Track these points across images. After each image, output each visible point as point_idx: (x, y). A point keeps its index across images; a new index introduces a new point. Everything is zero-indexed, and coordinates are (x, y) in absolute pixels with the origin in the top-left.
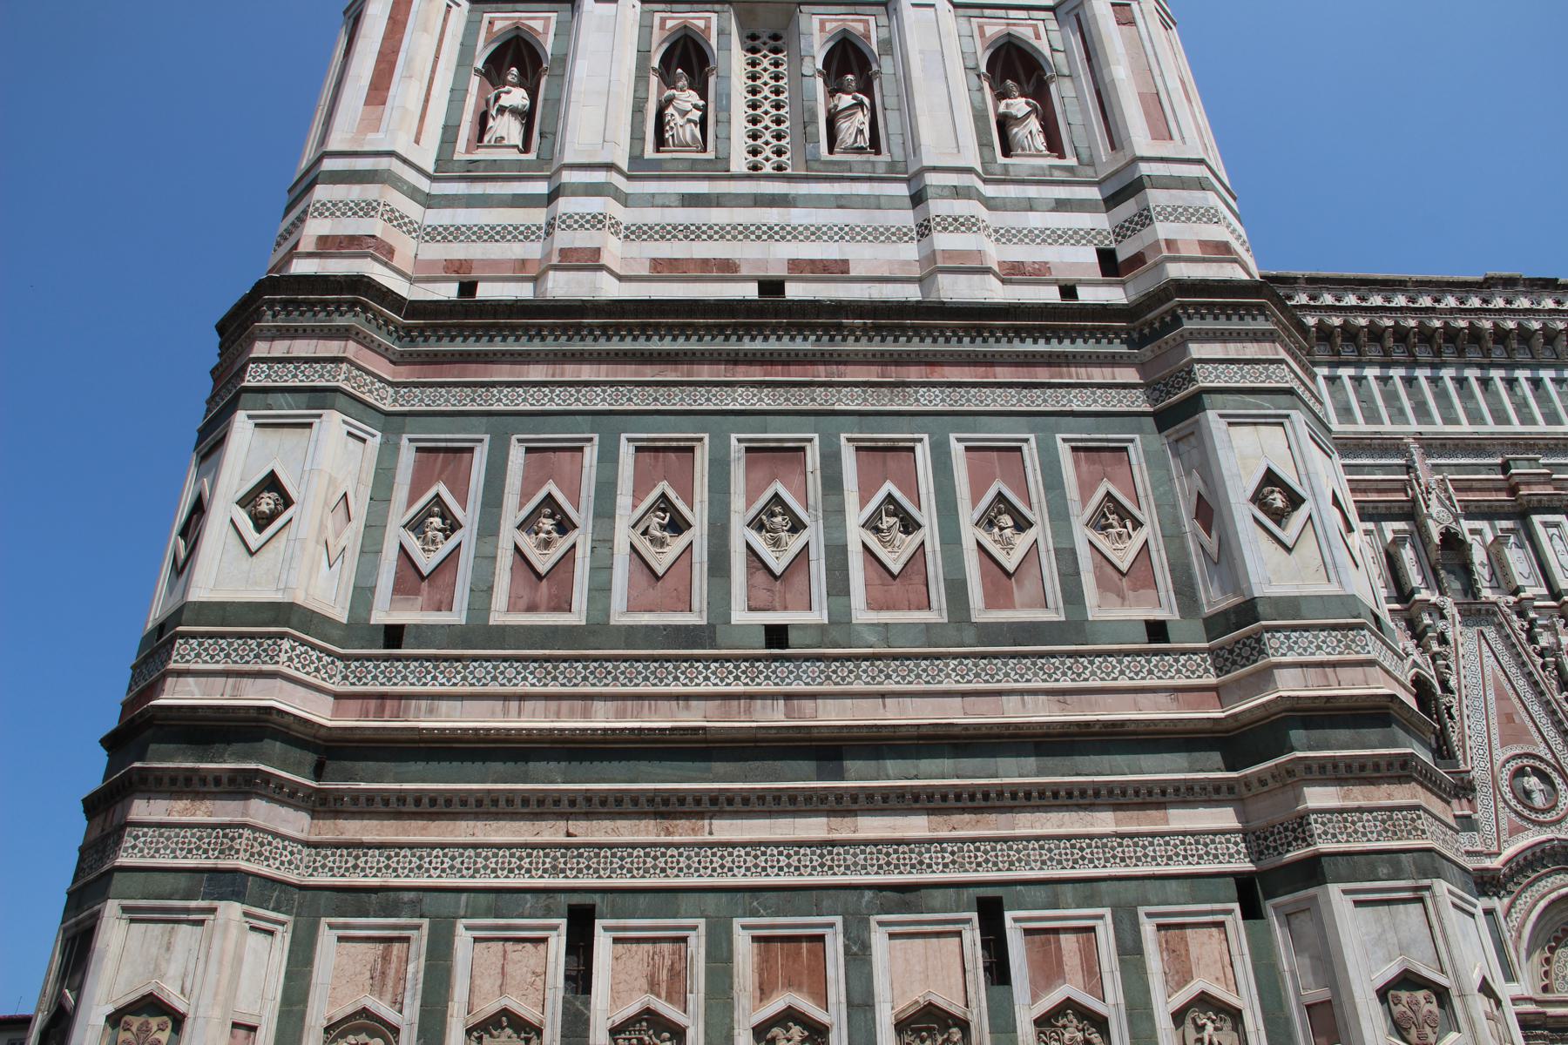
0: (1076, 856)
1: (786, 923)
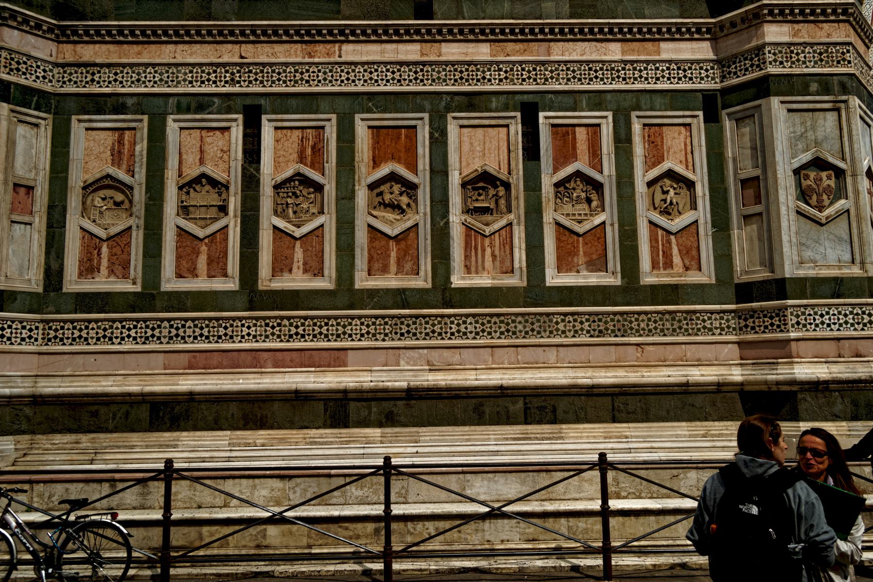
0: (592, 76)
1: (390, 119)
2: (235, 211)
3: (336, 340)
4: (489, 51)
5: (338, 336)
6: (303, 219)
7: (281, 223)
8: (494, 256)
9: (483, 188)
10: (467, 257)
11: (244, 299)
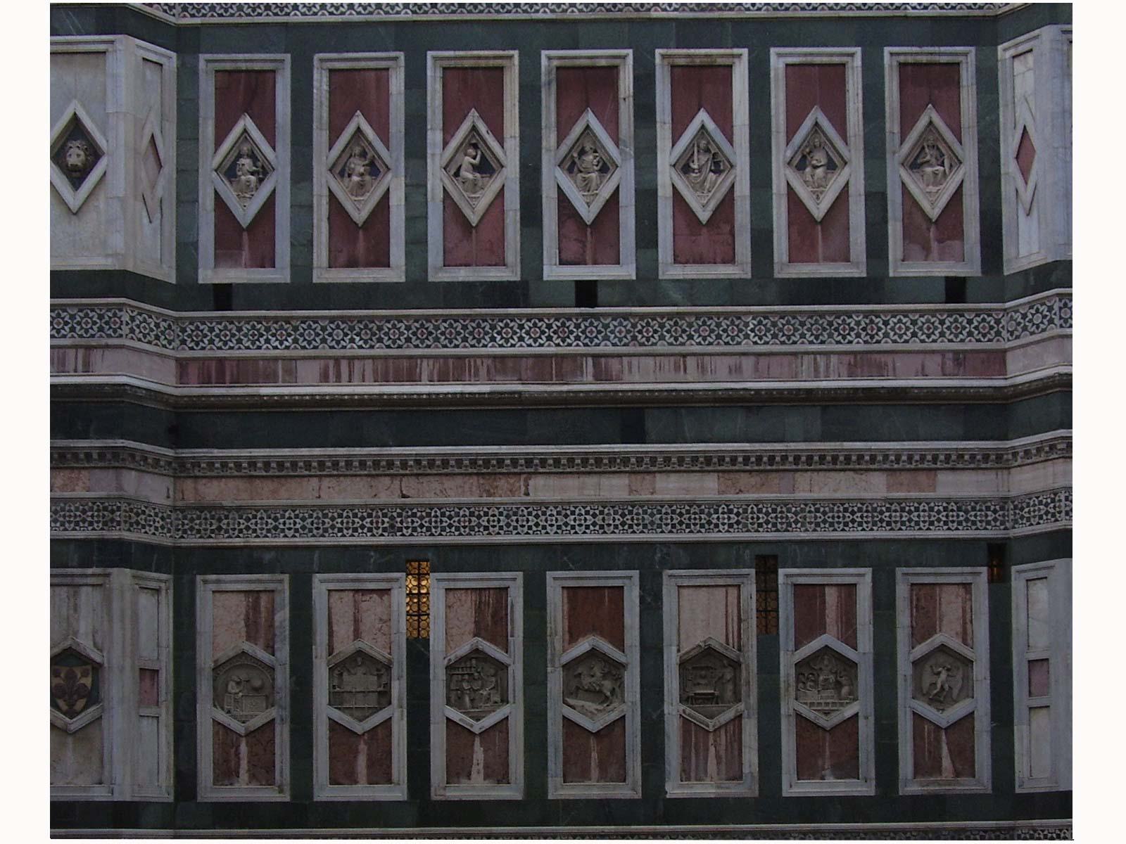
2: (400, 699)
8: (718, 757)
9: (708, 668)
10: (685, 759)
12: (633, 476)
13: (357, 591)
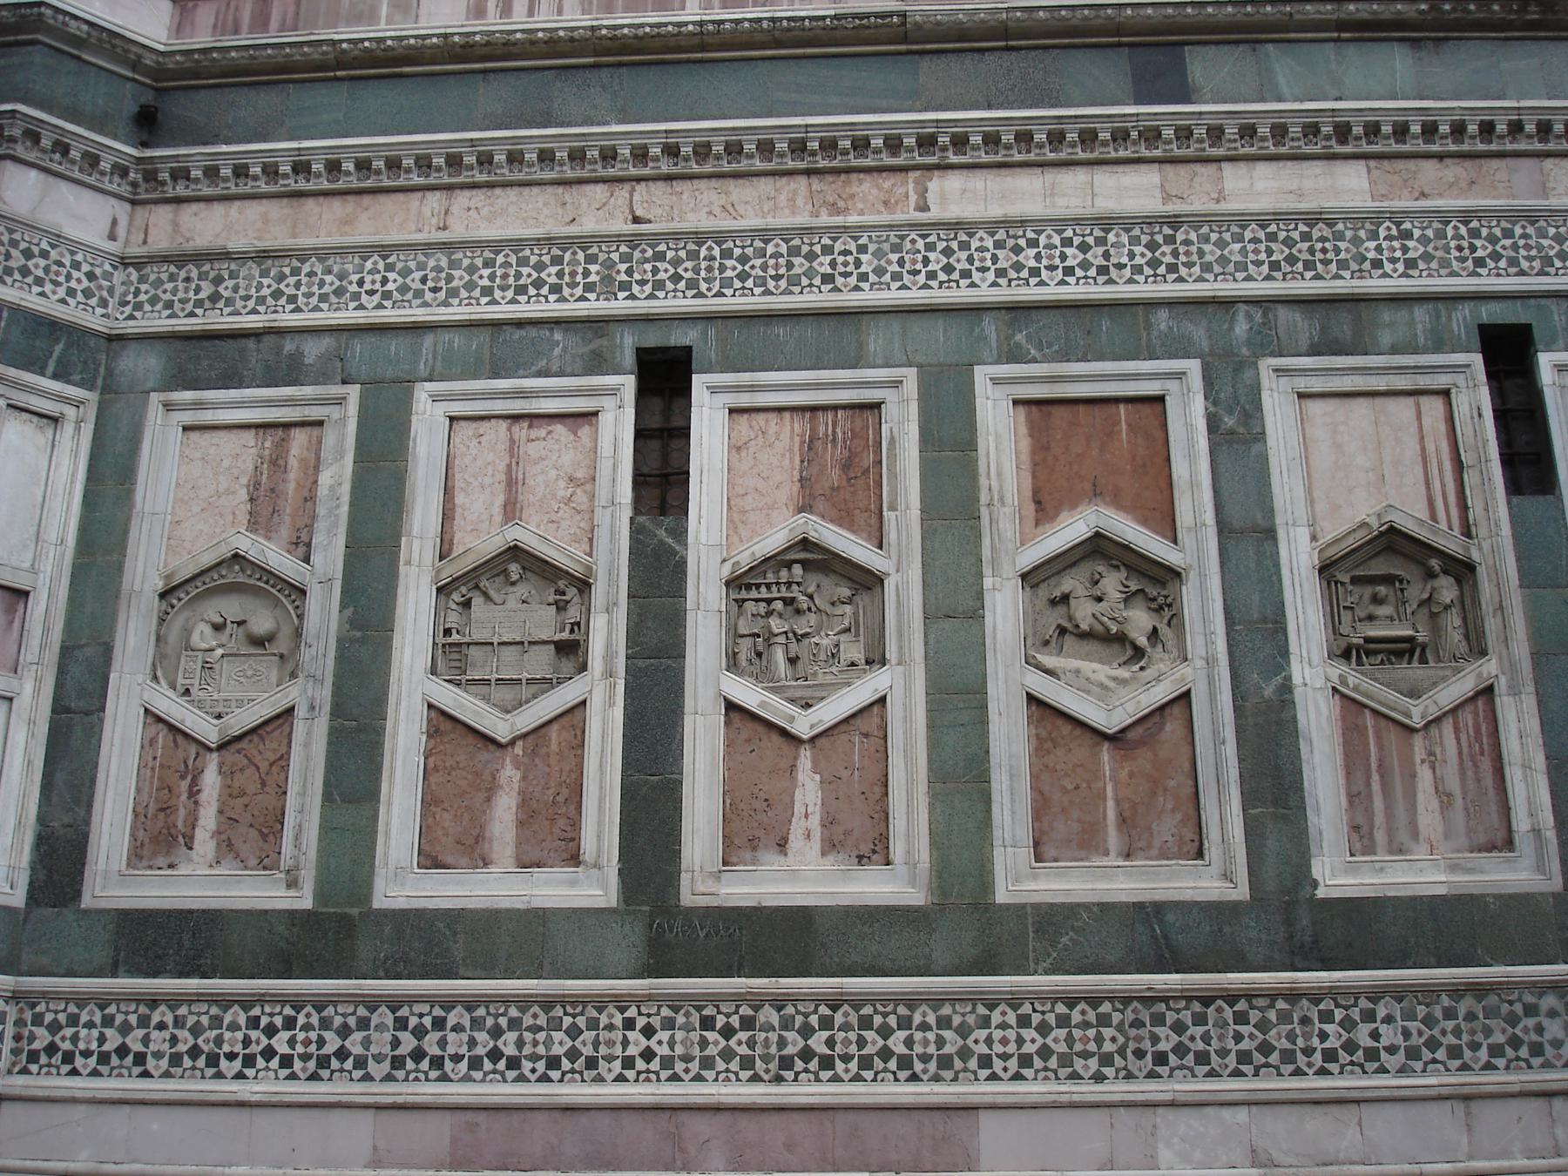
2: (609, 656)
3: (936, 1079)
4: (1366, 185)
5: (945, 1062)
6: (821, 679)
7: (748, 694)
9: (1389, 580)
10: (1356, 798)
11: (628, 940)
12: (1168, 168)
13: (516, 418)
